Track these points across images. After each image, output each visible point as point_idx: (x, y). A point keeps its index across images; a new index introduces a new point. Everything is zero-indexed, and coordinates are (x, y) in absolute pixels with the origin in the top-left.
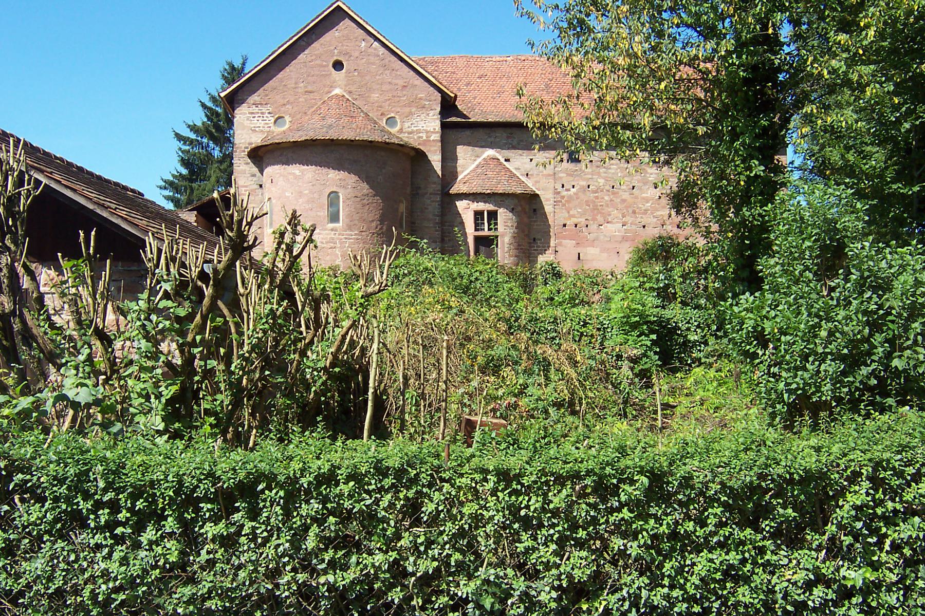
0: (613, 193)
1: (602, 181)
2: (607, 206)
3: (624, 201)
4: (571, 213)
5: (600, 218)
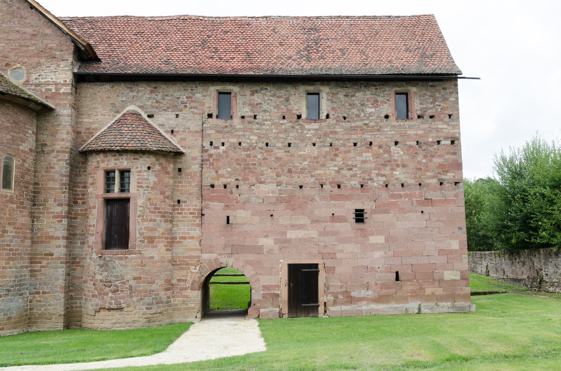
0: (267, 151)
2: (260, 165)
3: (278, 159)
4: (220, 172)
5: (252, 179)
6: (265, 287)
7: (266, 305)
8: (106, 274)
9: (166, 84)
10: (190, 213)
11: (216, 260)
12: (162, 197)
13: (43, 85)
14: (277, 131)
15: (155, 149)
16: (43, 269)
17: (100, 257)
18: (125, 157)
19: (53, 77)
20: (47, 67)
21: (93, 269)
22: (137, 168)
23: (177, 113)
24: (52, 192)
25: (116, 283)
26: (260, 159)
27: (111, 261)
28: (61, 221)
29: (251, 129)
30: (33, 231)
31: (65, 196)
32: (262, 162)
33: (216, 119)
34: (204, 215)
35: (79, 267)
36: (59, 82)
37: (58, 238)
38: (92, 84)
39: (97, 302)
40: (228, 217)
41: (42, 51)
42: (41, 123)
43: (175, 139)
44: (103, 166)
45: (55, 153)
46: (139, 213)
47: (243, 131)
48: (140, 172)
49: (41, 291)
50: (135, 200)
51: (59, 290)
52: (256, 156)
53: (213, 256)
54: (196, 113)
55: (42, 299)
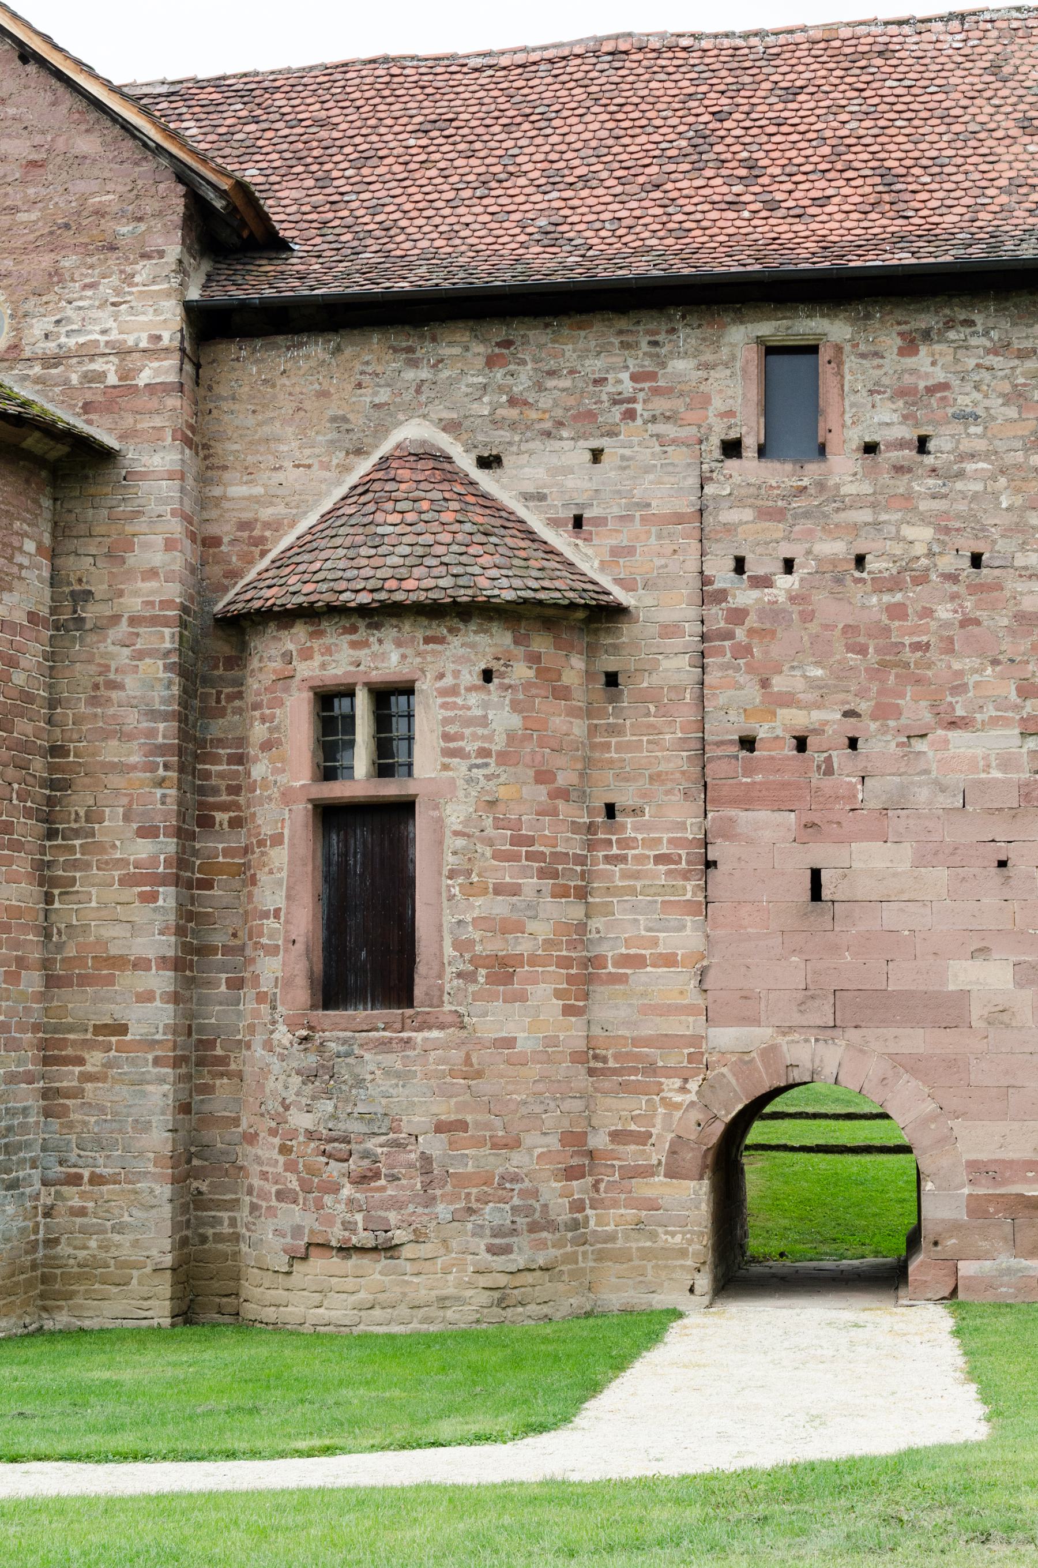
0: (975, 589)
1: (921, 535)
2: (949, 647)
4: (779, 683)
6: (978, 1170)
7: (985, 1245)
8: (329, 1106)
9: (547, 326)
10: (659, 859)
11: (770, 1052)
12: (542, 792)
13: (74, 360)
14: (1018, 501)
15: (509, 595)
16: (89, 1086)
17: (306, 1039)
18: (393, 633)
19: (111, 324)
20: (86, 287)
21: (280, 1086)
22: (441, 676)
23: (595, 444)
24: (115, 780)
25: (370, 1144)
26: (946, 625)
27: (348, 1055)
28: (153, 897)
29: (908, 497)
30: (48, 936)
31: (164, 796)
32: (958, 634)
33: (756, 462)
34: (714, 864)
35: (225, 1081)
36: (131, 343)
37: (140, 964)
38: (259, 343)
39: (298, 1220)
40: (816, 875)
41: (67, 226)
42: (70, 511)
43: (590, 552)
44: (306, 674)
45: (124, 627)
46: (450, 859)
47: (874, 506)
48: (453, 691)
49: (86, 1174)
50: (436, 807)
51: (152, 1169)
52: (928, 613)
53: (761, 1035)
54: (674, 442)
55: (91, 1205)
